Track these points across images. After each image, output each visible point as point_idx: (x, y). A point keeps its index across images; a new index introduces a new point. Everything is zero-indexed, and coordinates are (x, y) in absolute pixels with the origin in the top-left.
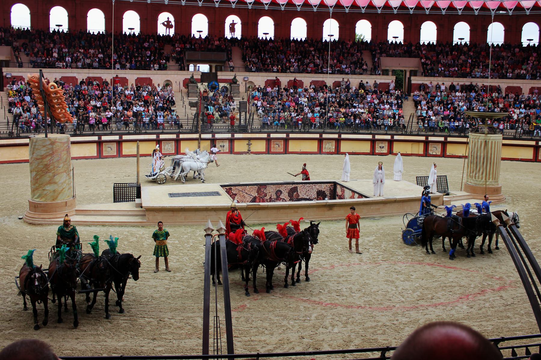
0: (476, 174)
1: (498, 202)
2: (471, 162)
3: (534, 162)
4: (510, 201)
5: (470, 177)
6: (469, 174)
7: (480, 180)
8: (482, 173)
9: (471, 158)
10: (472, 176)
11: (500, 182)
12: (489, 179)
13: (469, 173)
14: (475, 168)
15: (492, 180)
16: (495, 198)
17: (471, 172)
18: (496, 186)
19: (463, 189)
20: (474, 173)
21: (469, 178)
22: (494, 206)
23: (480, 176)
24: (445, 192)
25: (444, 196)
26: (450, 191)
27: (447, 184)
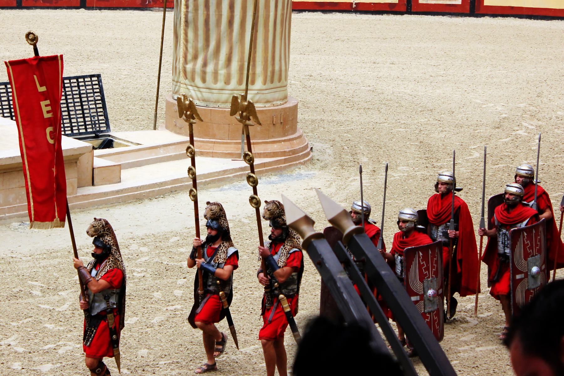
0: (205, 65)
1: (285, 161)
2: (186, 21)
3: (402, 13)
4: (328, 158)
5: (186, 78)
6: (180, 65)
7: (220, 84)
8: (229, 60)
9: (187, 6)
10: (193, 72)
11: (290, 90)
12: (253, 83)
13: (182, 60)
14: (201, 44)
15: (265, 83)
16: (276, 148)
17: (189, 57)
18: (279, 105)
19: (160, 121)
20: (200, 61)
21: (182, 79)
22: (274, 178)
23: (222, 72)
24: (97, 137)
25: (97, 152)
26: (114, 133)
27: (104, 107)
